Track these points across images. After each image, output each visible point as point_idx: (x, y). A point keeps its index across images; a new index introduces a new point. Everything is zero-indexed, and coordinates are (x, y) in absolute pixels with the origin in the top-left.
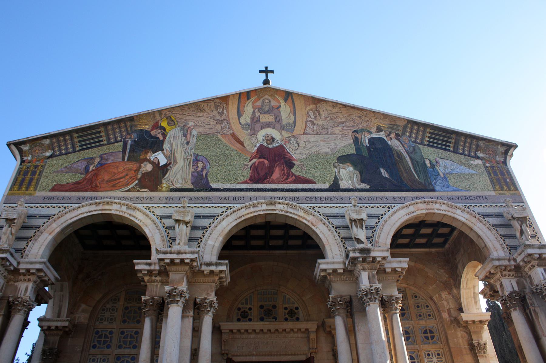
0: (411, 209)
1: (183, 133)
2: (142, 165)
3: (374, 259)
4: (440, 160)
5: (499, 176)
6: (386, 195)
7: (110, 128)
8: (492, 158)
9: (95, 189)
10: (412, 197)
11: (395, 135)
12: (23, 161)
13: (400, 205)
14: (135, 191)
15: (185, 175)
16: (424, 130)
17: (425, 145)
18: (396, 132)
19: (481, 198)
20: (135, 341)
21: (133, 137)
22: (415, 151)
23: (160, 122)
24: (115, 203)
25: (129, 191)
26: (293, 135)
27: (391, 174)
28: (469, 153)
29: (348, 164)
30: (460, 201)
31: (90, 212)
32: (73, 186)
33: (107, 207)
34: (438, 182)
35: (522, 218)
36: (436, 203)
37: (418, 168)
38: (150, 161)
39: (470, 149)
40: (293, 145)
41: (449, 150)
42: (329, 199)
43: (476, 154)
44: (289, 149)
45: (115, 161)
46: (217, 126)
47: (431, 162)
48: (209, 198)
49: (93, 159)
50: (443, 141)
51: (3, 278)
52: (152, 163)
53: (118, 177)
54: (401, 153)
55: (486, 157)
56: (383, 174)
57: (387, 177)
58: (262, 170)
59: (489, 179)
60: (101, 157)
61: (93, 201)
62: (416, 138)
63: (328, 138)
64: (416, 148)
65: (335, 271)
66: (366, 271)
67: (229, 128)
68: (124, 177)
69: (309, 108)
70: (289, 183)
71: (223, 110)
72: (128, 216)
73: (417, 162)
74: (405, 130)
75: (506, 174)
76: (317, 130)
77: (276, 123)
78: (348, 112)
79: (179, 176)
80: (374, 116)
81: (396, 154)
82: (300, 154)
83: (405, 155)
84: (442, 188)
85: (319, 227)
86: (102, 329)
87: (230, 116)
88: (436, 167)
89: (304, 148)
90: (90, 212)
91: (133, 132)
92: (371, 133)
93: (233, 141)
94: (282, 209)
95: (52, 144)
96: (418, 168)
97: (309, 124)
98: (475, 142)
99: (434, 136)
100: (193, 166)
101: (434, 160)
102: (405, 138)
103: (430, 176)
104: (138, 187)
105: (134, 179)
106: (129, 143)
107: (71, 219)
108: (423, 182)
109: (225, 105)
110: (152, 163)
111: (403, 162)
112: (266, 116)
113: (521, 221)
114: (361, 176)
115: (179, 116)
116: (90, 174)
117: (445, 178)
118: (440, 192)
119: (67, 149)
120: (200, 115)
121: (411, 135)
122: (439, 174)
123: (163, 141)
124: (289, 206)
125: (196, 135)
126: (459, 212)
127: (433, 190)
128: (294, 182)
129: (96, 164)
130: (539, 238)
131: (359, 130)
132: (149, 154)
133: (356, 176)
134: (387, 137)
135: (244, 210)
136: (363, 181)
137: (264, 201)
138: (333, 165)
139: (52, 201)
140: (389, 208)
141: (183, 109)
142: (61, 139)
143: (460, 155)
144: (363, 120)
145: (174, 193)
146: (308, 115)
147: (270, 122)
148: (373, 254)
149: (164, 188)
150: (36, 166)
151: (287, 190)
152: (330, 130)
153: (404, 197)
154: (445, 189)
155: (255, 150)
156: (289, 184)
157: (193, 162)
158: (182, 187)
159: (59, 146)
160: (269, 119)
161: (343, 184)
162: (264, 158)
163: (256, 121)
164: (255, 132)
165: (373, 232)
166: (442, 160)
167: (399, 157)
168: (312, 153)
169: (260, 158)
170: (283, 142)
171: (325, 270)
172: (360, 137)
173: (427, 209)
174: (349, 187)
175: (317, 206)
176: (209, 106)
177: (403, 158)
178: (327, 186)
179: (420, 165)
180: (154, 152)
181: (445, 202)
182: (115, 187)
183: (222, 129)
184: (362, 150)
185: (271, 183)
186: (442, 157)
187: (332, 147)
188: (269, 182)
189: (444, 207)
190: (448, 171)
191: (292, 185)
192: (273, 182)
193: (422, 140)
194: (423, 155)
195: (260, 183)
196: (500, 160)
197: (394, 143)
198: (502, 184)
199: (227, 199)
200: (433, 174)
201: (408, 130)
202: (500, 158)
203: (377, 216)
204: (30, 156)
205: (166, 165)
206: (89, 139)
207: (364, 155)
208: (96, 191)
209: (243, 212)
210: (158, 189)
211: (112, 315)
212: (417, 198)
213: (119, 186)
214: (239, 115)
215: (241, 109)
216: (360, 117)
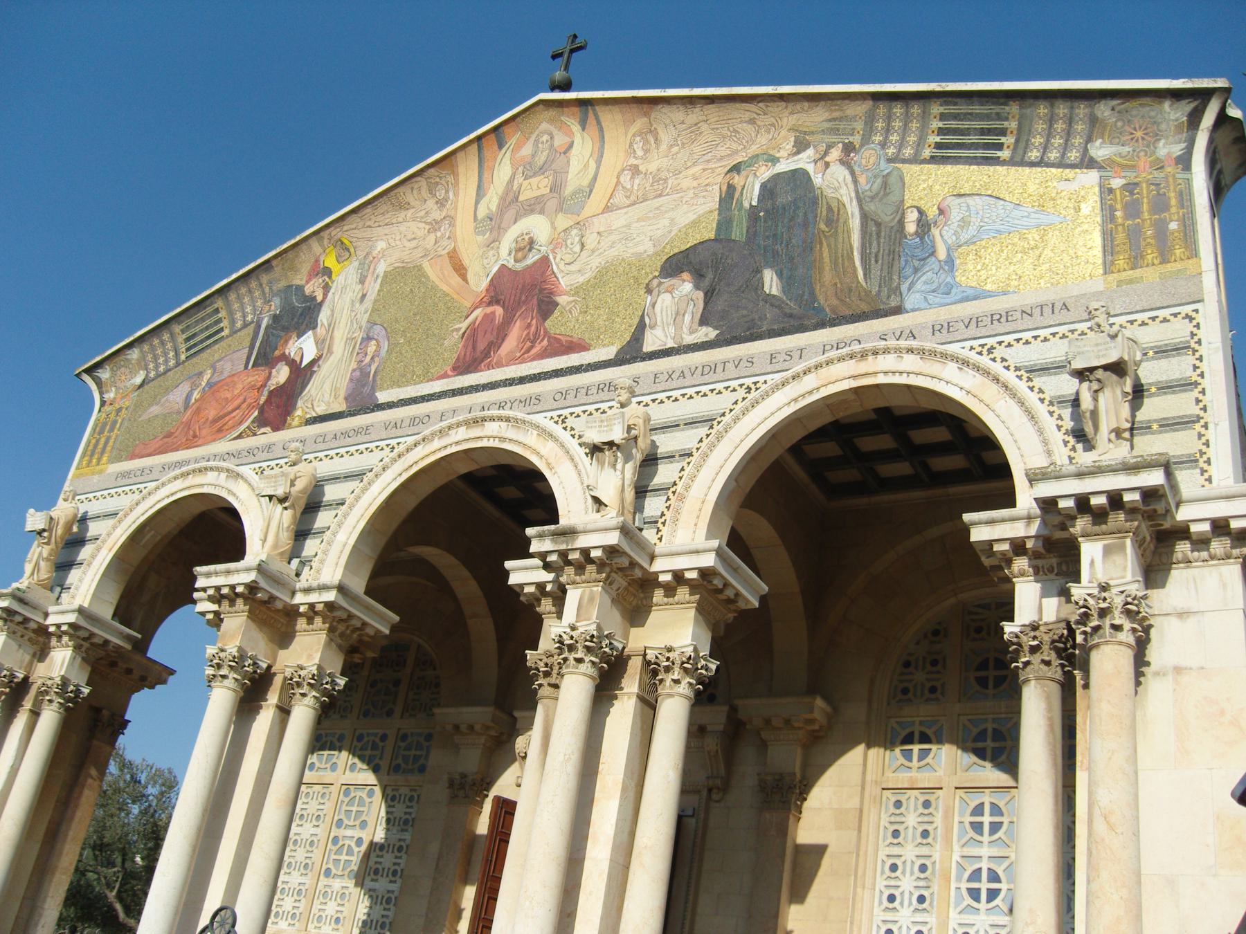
0: (810, 381)
1: (361, 274)
2: (274, 371)
3: (585, 552)
4: (954, 203)
5: (1146, 215)
6: (755, 351)
7: (232, 296)
8: (1142, 154)
10: (824, 346)
11: (842, 152)
12: (103, 403)
13: (778, 377)
14: (248, 436)
15: (339, 380)
16: (924, 112)
17: (925, 161)
18: (847, 141)
19: (1047, 310)
20: (378, 757)
21: (273, 308)
22: (885, 189)
23: (322, 259)
24: (211, 469)
25: (239, 437)
26: (579, 219)
28: (1063, 155)
29: (686, 275)
30: (972, 331)
31: (172, 494)
32: (161, 442)
33: (198, 479)
34: (923, 279)
35: (1106, 368)
36: (886, 351)
37: (875, 244)
39: (1067, 141)
40: (571, 249)
41: (995, 161)
42: (606, 389)
43: (1086, 150)
45: (233, 373)
46: (428, 239)
47: (919, 221)
48: (366, 430)
50: (983, 132)
51: (28, 643)
53: (230, 408)
54: (841, 204)
55: (1120, 155)
56: (767, 290)
57: (775, 292)
58: (485, 334)
59: (1104, 233)
60: (213, 367)
61: (178, 472)
62: (901, 144)
63: (657, 208)
64: (892, 180)
65: (541, 586)
66: (577, 588)
67: (449, 238)
68: (238, 408)
69: (634, 129)
70: (531, 360)
71: (447, 192)
72: (224, 494)
73: (878, 225)
74: (871, 128)
75: (1173, 202)
76: (638, 190)
77: (551, 195)
78: (721, 114)
79: (327, 387)
80: (786, 107)
81: (824, 213)
82: (579, 271)
83: (853, 209)
84: (926, 299)
85: (558, 471)
86: (328, 731)
87: (460, 205)
88: (933, 230)
89: (593, 251)
90: (172, 494)
91: (273, 297)
92: (774, 160)
93: (449, 270)
94: (495, 434)
95: (143, 356)
96: (875, 244)
97: (626, 178)
98: (1082, 109)
99: (953, 124)
100: (358, 353)
101: (936, 207)
103: (903, 263)
104: (255, 425)
105: (254, 406)
107: (143, 514)
108: (874, 293)
109: (451, 179)
111: (836, 240)
112: (534, 181)
113: (1099, 380)
114: (706, 303)
115: (356, 233)
116: (189, 412)
117: (950, 261)
118: (917, 313)
119: (166, 362)
120: (400, 219)
121: (887, 137)
122: (933, 254)
123: (321, 304)
124: (510, 424)
125: (382, 275)
126: (951, 370)
127: (898, 310)
129: (203, 384)
130: (1211, 426)
131: (745, 162)
132: (291, 342)
133: (692, 307)
134: (815, 162)
135: (419, 448)
136: (704, 321)
137: (461, 418)
138: (647, 285)
139: (127, 481)
140: (749, 389)
141: (364, 213)
142: (156, 342)
143: (1027, 170)
144: (759, 126)
145: (309, 427)
147: (537, 197)
148: (582, 542)
149: (297, 419)
150: (119, 410)
151: (522, 380)
152: (670, 182)
153: (801, 350)
154: (937, 300)
155: (485, 283)
156: (529, 364)
157: (361, 344)
158: (326, 410)
159: (155, 358)
160: (539, 188)
162: (498, 302)
163: (510, 203)
164: (499, 233)
165: (682, 469)
166: (962, 200)
167: (829, 222)
168: (608, 262)
169: (490, 304)
170: (551, 247)
171: (522, 586)
172: (742, 184)
173: (855, 377)
174: (665, 345)
175: (571, 414)
176: (415, 192)
177: (841, 221)
178: (609, 353)
180: (299, 337)
181: (914, 344)
183: (436, 243)
184: (735, 224)
185: (493, 368)
186: (962, 192)
187: (659, 233)
189: (910, 362)
190: (965, 237)
191: (535, 363)
192: (500, 365)
193: (919, 145)
194: (906, 198)
195: (471, 372)
196: (1168, 153)
198: (1143, 243)
199: (398, 426)
200: (913, 257)
201: (880, 125)
202: (1169, 148)
203: (709, 421)
204: (113, 389)
205: (313, 362)
206: (202, 331)
207: (733, 238)
208: (191, 448)
209: (419, 452)
210: (287, 424)
211: (348, 699)
213: (227, 430)
215: (486, 175)
216: (752, 121)
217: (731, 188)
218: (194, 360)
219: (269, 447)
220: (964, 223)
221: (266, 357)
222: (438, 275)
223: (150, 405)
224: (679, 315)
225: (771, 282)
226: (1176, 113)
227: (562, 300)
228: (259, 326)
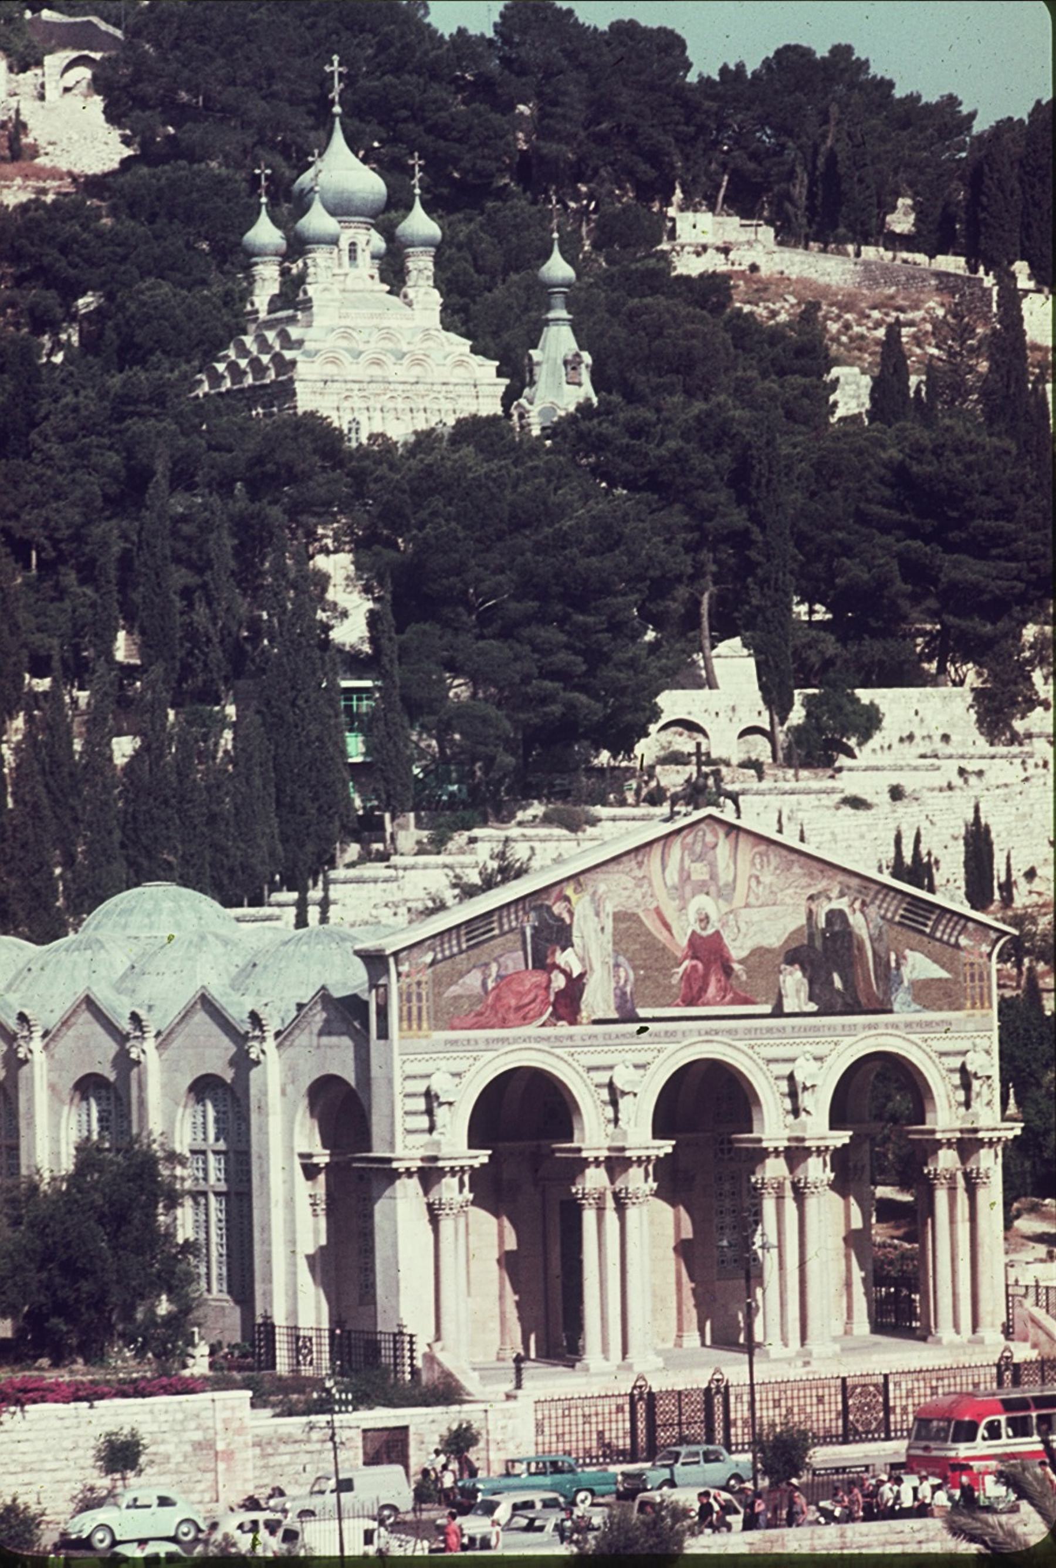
4: (907, 952)
9: (504, 1024)
12: (399, 974)
25: (543, 1025)
38: (558, 967)
44: (727, 940)
52: (563, 971)
60: (496, 960)
68: (533, 1001)
79: (599, 997)
92: (829, 899)
93: (659, 924)
97: (753, 883)
102: (872, 911)
106: (529, 932)
110: (563, 971)
112: (698, 865)
123: (570, 926)
126: (914, 1049)
127: (891, 1011)
128: (733, 1002)
132: (558, 952)
136: (811, 998)
146: (753, 864)
150: (419, 983)
152: (780, 896)
155: (684, 942)
161: (788, 1006)
178: (767, 1009)
180: (563, 949)
182: (525, 1020)
188: (704, 1004)
189: (899, 1042)
190: (916, 975)
197: (856, 921)
202: (985, 948)
205: (582, 976)
212: (870, 1027)
214: (664, 868)
217: (810, 912)
218: (476, 951)
219: (571, 1037)
220: (914, 968)
221: (542, 963)
222: (651, 924)
223: (450, 985)
224: (798, 991)
225: (838, 983)
226: (993, 935)
227: (736, 967)
228: (524, 934)
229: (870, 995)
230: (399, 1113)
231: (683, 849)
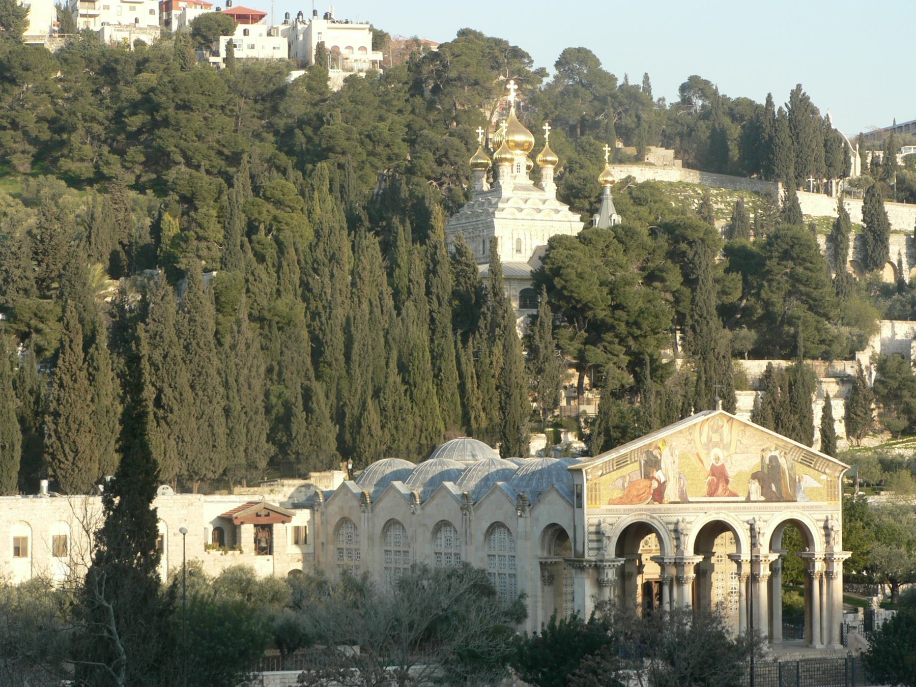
9: (631, 503)
27: (777, 488)
49: (624, 477)
102: (789, 456)
106: (643, 462)
112: (715, 435)
127: (796, 501)
128: (728, 496)
155: (709, 469)
161: (753, 498)
169: (713, 475)
178: (744, 499)
179: (793, 480)
182: (641, 501)
192: (718, 496)
197: (782, 461)
205: (665, 482)
218: (620, 470)
219: (660, 509)
221: (648, 476)
225: (774, 489)
227: (730, 480)
229: (787, 494)
230: (586, 541)
231: (709, 427)
